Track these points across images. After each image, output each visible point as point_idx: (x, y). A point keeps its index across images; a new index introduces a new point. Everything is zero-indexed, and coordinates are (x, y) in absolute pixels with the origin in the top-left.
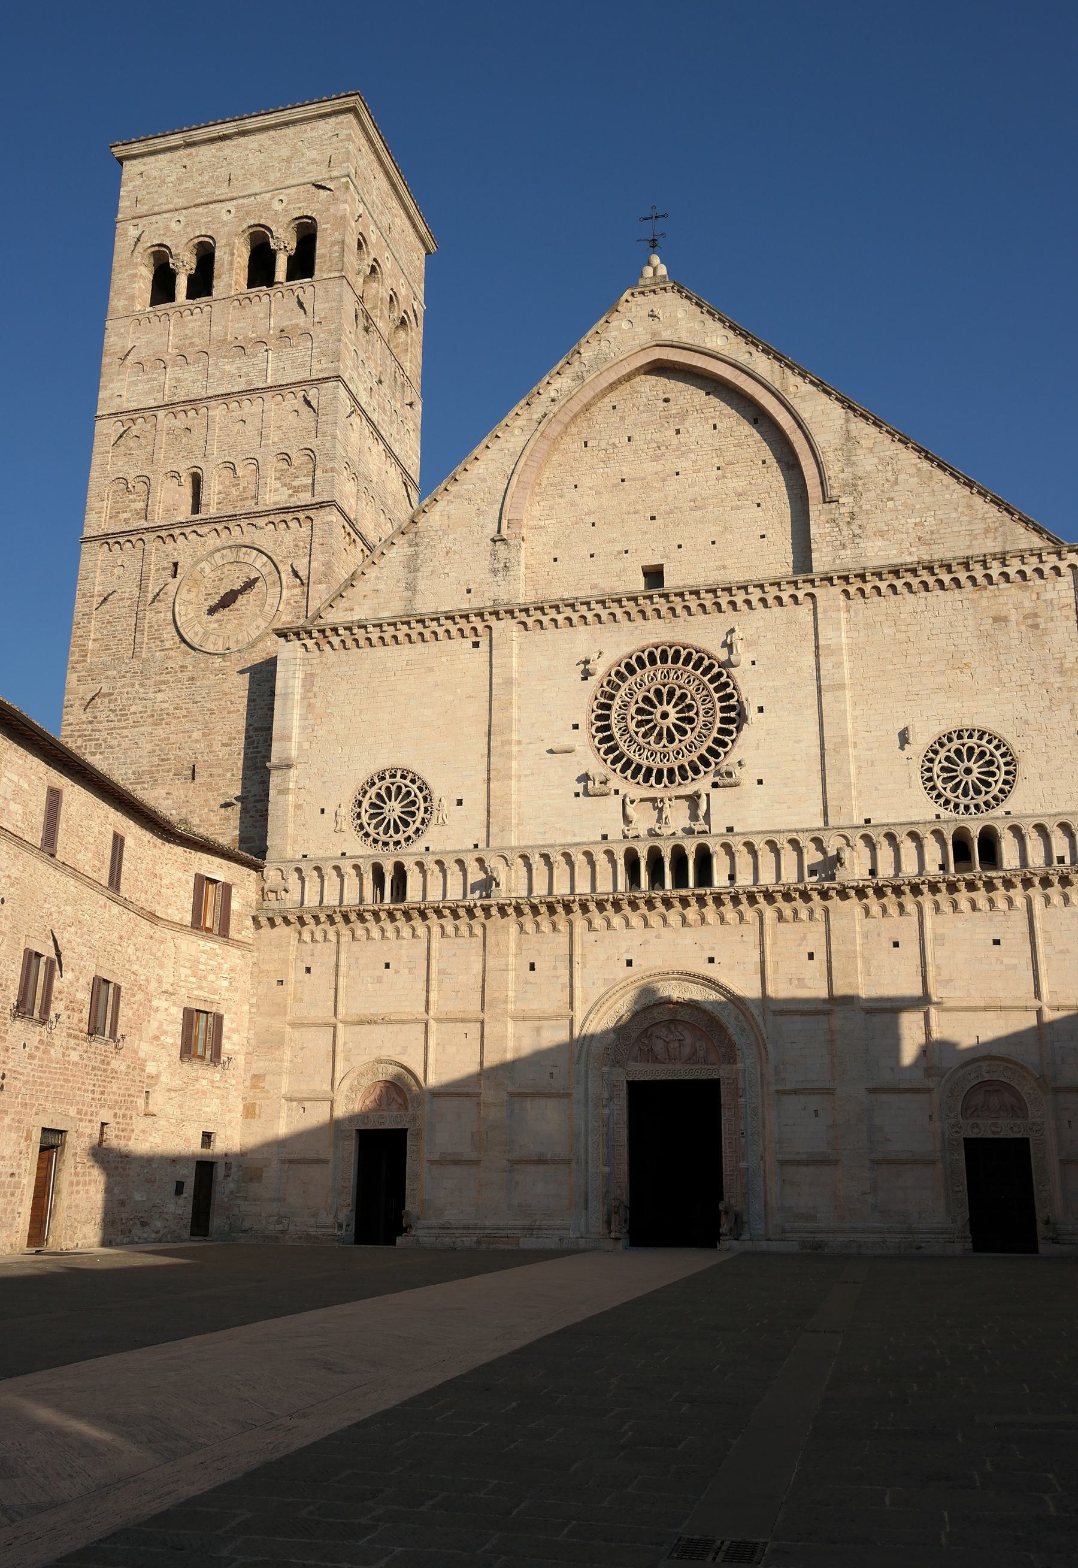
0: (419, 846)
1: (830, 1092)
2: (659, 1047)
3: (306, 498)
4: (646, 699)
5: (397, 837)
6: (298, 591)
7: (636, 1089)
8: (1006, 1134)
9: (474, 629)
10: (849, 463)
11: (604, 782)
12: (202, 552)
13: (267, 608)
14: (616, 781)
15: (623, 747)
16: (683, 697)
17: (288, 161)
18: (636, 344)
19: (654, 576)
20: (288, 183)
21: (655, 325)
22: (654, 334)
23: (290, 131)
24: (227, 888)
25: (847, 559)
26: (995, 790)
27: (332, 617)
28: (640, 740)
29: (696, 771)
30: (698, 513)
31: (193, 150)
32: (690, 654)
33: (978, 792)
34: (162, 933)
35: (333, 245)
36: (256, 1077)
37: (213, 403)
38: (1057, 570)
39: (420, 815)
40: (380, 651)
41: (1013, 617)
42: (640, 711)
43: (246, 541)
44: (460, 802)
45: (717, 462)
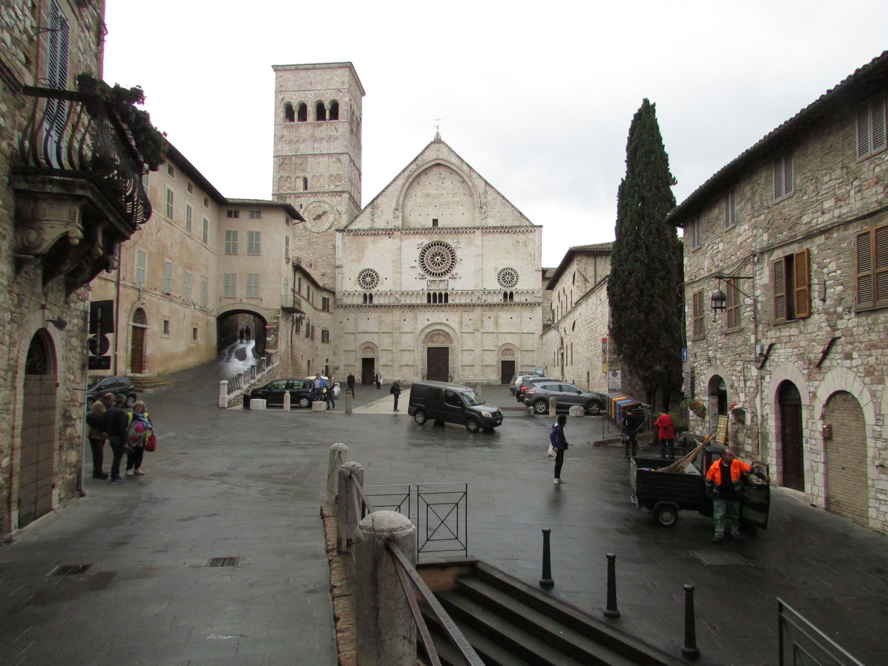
0: (376, 289)
1: (473, 350)
2: (435, 340)
3: (339, 189)
4: (433, 255)
5: (370, 287)
6: (338, 216)
7: (429, 349)
8: (510, 360)
9: (389, 233)
10: (486, 198)
11: (423, 276)
12: (310, 202)
13: (329, 220)
14: (426, 276)
15: (427, 267)
16: (443, 255)
17: (330, 80)
18: (432, 158)
19: (435, 222)
20: (330, 88)
21: (439, 154)
22: (437, 156)
23: (329, 70)
24: (328, 299)
25: (484, 223)
26: (514, 283)
27: (352, 227)
28: (432, 265)
29: (445, 274)
30: (447, 206)
31: (299, 71)
32: (444, 244)
33: (510, 283)
34: (318, 312)
35: (345, 110)
36: (336, 346)
37: (310, 157)
38: (531, 231)
39: (376, 281)
40: (364, 238)
41: (521, 241)
42: (432, 258)
43: (321, 200)
44: (386, 279)
45: (452, 192)
